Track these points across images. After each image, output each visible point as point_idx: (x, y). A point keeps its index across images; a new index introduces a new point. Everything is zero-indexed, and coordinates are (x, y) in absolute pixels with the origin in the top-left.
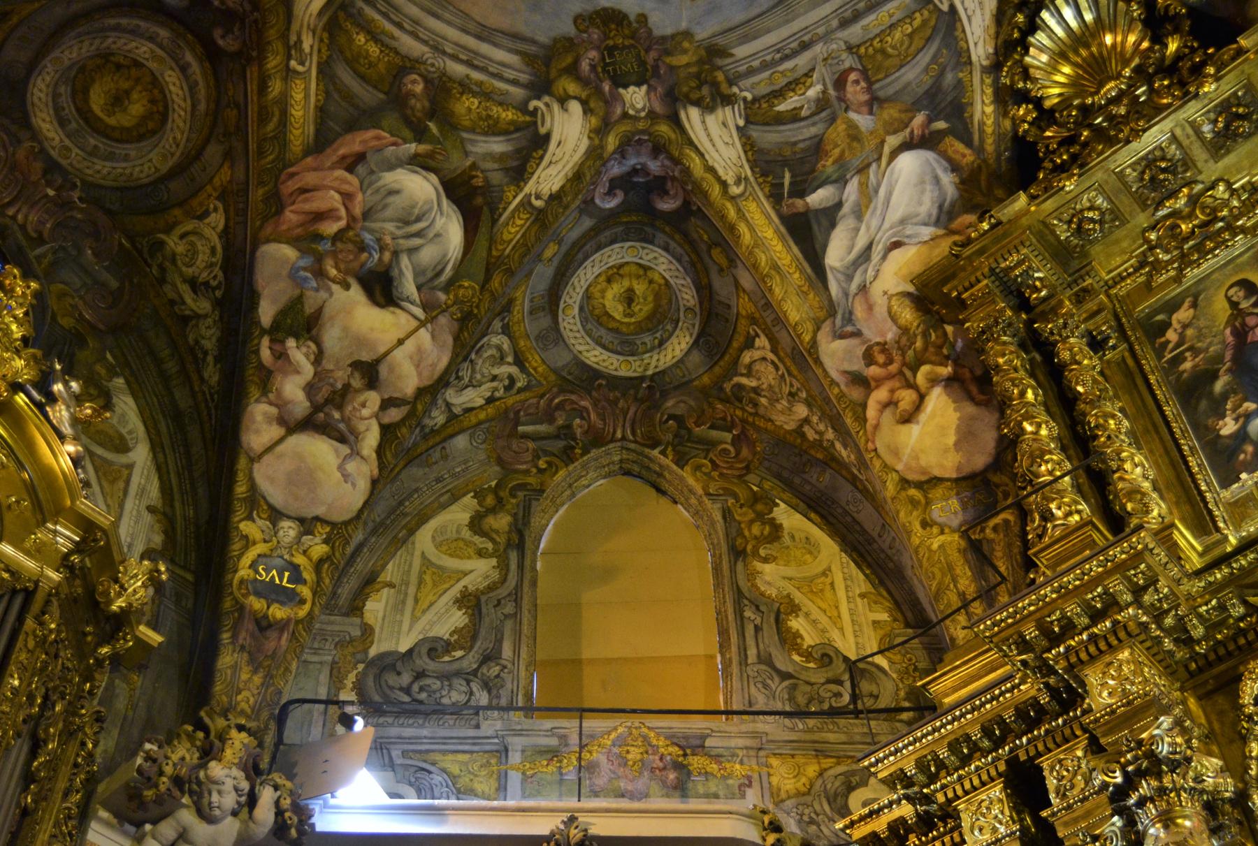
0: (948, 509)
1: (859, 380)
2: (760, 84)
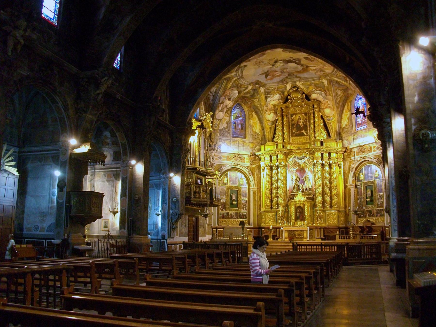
0: (270, 124)
1: (266, 110)
2: (268, 87)
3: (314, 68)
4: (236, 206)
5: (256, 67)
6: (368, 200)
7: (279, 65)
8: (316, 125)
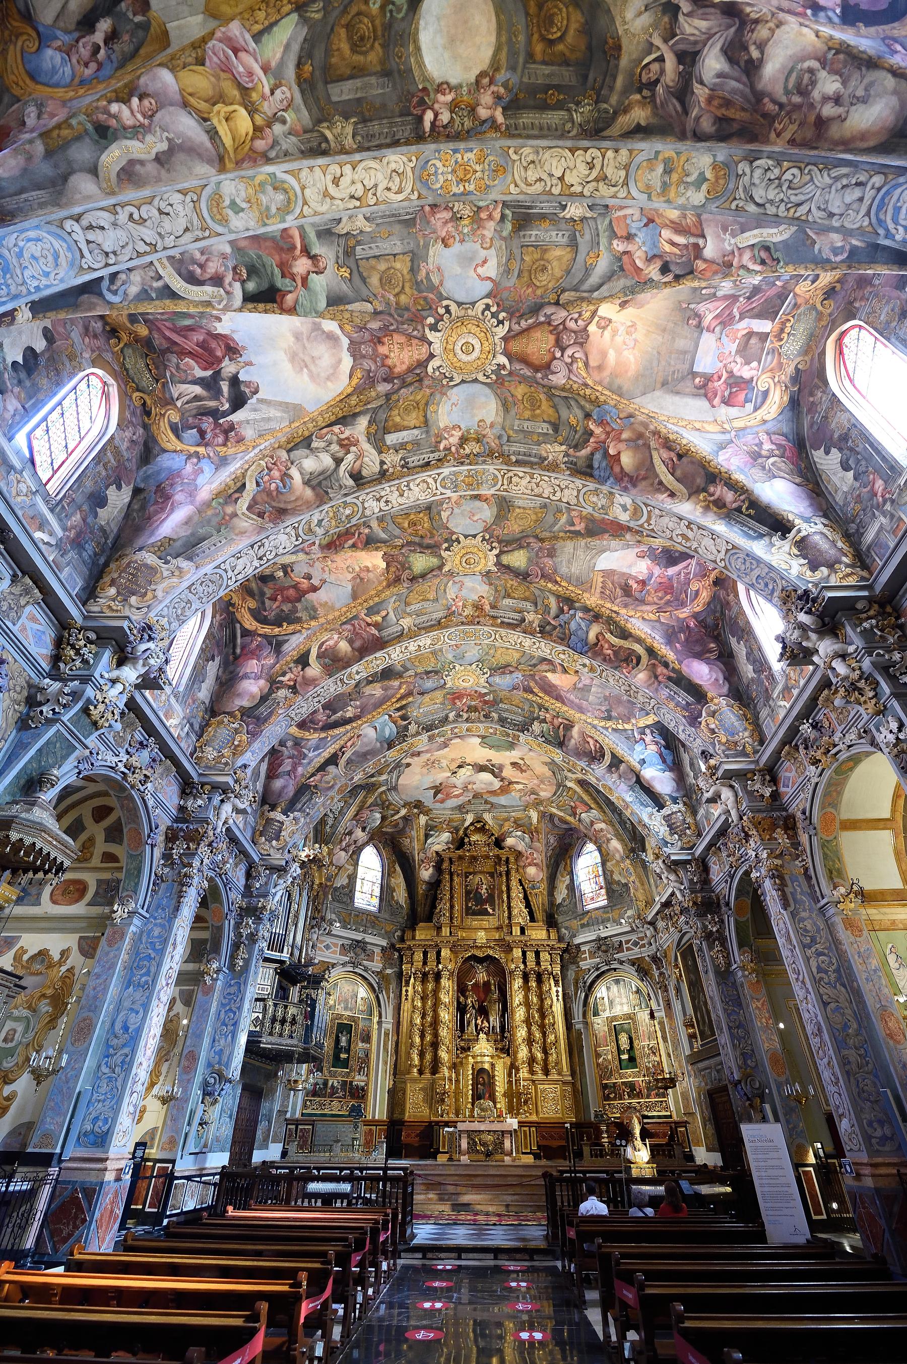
3: (520, 787)
4: (345, 1064)
5: (425, 770)
6: (625, 1057)
7: (465, 772)
8: (513, 895)
